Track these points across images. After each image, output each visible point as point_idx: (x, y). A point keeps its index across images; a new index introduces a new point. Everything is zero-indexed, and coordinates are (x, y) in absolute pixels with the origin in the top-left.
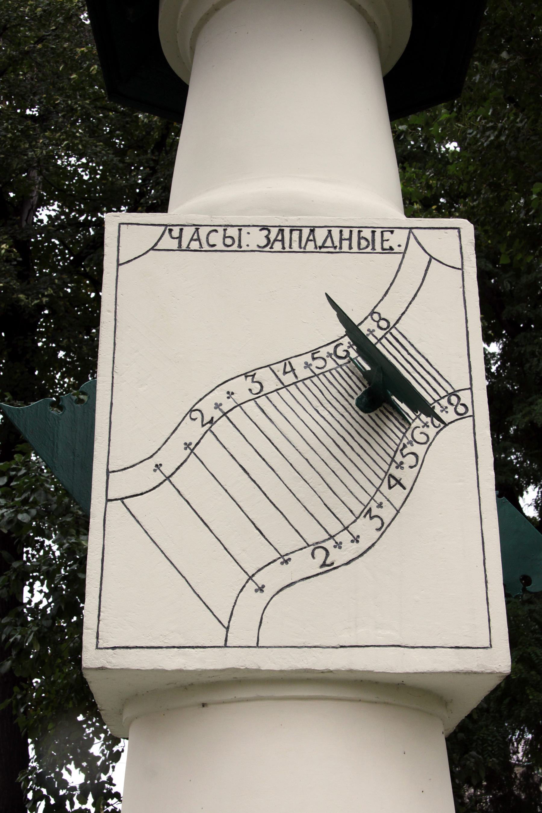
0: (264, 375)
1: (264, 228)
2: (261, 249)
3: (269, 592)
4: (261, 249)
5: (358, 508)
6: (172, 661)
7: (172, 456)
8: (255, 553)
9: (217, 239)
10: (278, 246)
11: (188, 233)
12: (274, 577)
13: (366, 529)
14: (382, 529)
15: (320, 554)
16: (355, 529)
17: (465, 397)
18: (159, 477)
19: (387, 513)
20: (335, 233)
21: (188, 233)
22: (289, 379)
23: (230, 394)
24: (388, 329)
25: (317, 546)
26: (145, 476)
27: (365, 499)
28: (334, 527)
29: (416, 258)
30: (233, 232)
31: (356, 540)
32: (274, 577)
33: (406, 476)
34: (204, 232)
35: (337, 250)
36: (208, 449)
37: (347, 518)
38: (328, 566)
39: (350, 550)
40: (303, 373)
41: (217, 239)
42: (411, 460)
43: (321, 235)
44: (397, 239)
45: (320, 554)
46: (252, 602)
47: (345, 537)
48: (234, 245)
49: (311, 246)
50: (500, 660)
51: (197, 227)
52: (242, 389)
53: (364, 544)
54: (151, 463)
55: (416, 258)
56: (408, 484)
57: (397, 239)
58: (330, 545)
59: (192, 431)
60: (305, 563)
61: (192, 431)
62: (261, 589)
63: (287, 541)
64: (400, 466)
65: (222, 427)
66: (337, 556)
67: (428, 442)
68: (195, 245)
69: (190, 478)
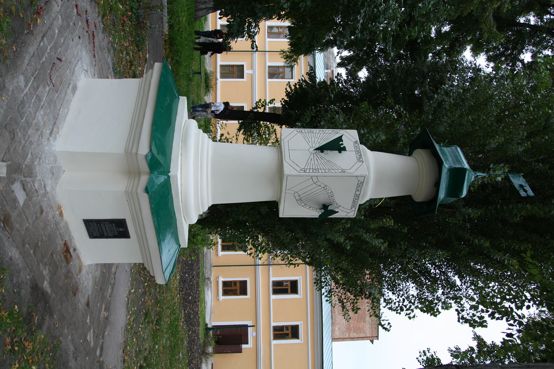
6: (284, 184)
7: (318, 183)
12: (296, 195)
13: (303, 204)
32: (296, 195)
33: (311, 209)
36: (319, 187)
39: (300, 203)
50: (281, 216)
55: (349, 211)
60: (298, 198)
61: (323, 186)
69: (315, 185)
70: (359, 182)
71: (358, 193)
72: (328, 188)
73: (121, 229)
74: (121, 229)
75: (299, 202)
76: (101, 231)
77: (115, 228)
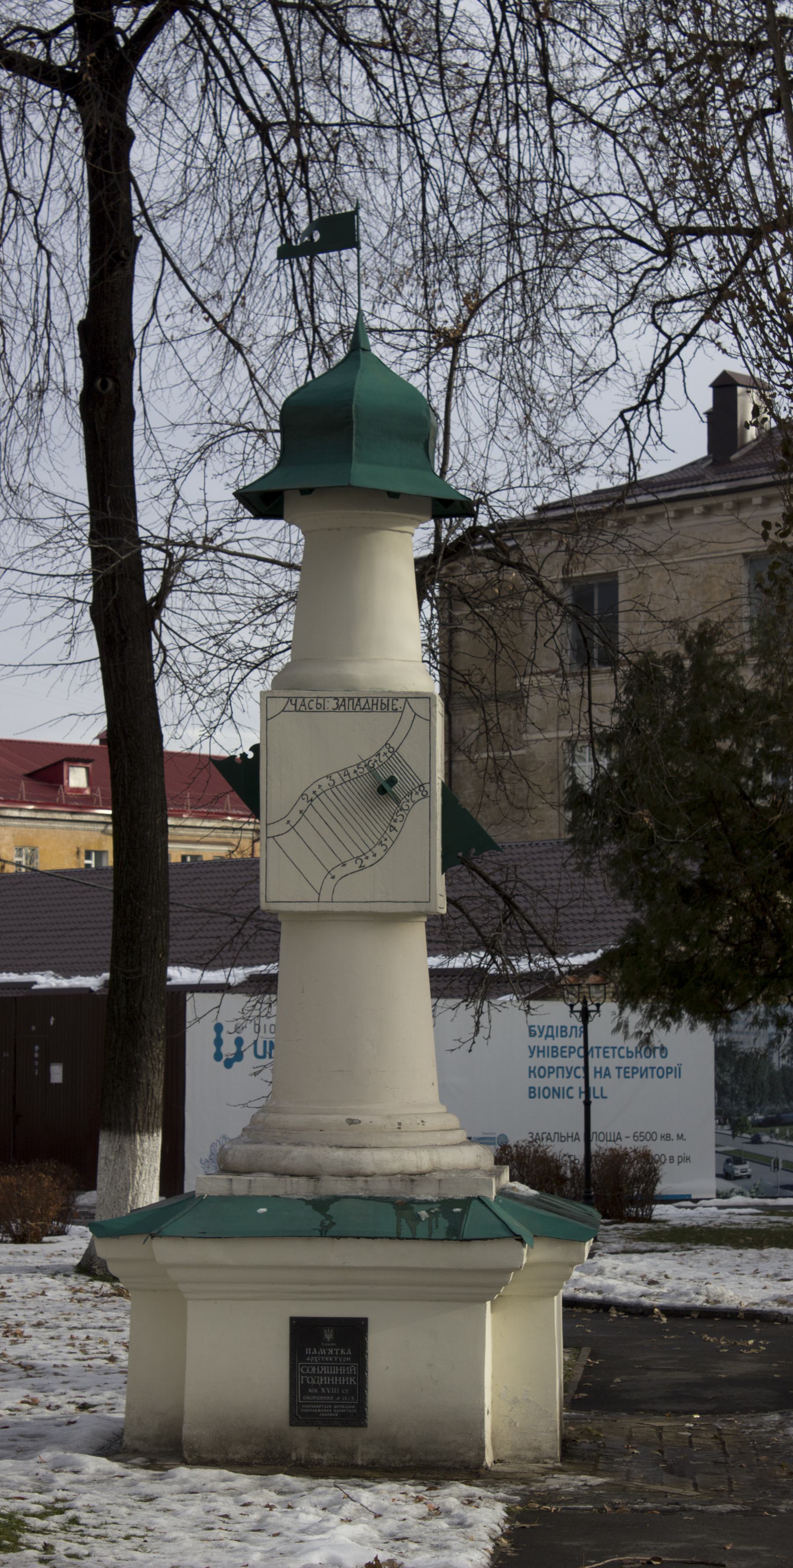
0: (336, 777)
1: (336, 698)
2: (334, 710)
3: (337, 878)
4: (334, 710)
5: (376, 841)
7: (294, 816)
8: (331, 862)
9: (313, 705)
10: (342, 708)
11: (300, 701)
12: (339, 872)
13: (379, 850)
14: (386, 850)
15: (359, 862)
16: (375, 850)
17: (427, 787)
18: (289, 827)
19: (388, 843)
20: (370, 701)
21: (300, 701)
22: (347, 778)
23: (320, 786)
24: (393, 753)
25: (358, 858)
26: (283, 827)
27: (379, 836)
28: (365, 850)
29: (408, 714)
30: (321, 701)
31: (375, 855)
33: (398, 826)
34: (307, 701)
35: (371, 710)
36: (310, 813)
37: (371, 845)
38: (362, 868)
39: (372, 860)
40: (353, 776)
41: (313, 705)
42: (400, 818)
43: (363, 702)
44: (399, 704)
45: (359, 862)
46: (330, 883)
47: (370, 854)
48: (321, 708)
49: (358, 708)
51: (304, 698)
52: (325, 783)
53: (378, 857)
54: (285, 820)
55: (408, 714)
56: (398, 829)
57: (399, 704)
58: (363, 858)
59: (303, 805)
60: (352, 866)
61: (303, 805)
62: (333, 877)
63: (345, 856)
64: (395, 821)
65: (316, 803)
66: (367, 863)
67: (409, 810)
68: (303, 708)
70: (290, 707)
71: (332, 704)
72: (315, 787)
73: (329, 1335)
74: (329, 1335)
75: (367, 863)
76: (335, 1391)
77: (323, 1352)
